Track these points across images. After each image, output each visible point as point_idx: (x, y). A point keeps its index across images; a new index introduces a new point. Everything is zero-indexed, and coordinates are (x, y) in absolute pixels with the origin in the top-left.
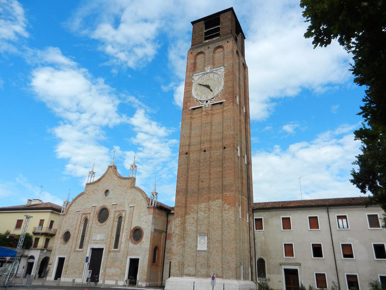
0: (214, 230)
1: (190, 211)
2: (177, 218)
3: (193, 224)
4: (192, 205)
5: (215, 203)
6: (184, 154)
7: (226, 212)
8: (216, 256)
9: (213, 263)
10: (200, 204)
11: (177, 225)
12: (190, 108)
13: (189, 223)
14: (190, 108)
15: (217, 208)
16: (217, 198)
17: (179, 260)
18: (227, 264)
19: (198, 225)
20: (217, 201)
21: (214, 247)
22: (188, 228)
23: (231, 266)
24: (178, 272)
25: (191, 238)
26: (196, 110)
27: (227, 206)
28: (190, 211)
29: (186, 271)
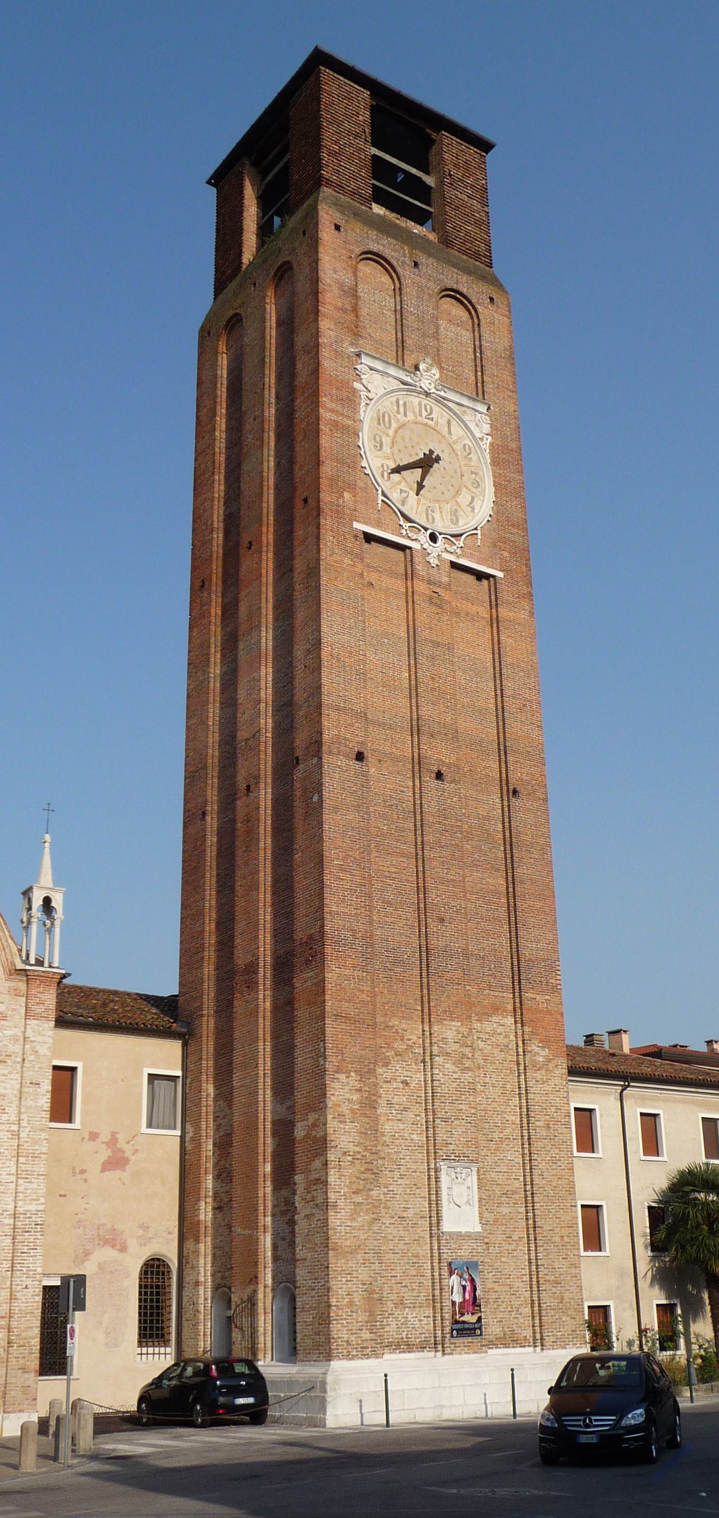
0: (493, 1146)
1: (389, 1046)
2: (342, 1077)
3: (406, 1109)
4: (395, 1022)
5: (488, 1027)
6: (346, 756)
7: (538, 1075)
8: (503, 1259)
9: (497, 1288)
10: (440, 1021)
11: (345, 1109)
12: (356, 525)
13: (389, 1103)
14: (356, 525)
15: (496, 1052)
16: (496, 1009)
17: (364, 1277)
18: (554, 1290)
19: (438, 1121)
20: (495, 1019)
21: (496, 1220)
22: (387, 1127)
23: (567, 1295)
24: (366, 1335)
25: (402, 1177)
26: (374, 545)
27: (542, 1053)
28: (389, 1046)
29: (391, 1328)
